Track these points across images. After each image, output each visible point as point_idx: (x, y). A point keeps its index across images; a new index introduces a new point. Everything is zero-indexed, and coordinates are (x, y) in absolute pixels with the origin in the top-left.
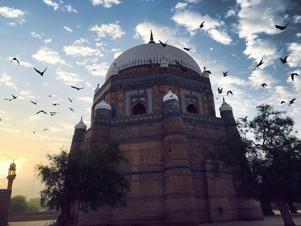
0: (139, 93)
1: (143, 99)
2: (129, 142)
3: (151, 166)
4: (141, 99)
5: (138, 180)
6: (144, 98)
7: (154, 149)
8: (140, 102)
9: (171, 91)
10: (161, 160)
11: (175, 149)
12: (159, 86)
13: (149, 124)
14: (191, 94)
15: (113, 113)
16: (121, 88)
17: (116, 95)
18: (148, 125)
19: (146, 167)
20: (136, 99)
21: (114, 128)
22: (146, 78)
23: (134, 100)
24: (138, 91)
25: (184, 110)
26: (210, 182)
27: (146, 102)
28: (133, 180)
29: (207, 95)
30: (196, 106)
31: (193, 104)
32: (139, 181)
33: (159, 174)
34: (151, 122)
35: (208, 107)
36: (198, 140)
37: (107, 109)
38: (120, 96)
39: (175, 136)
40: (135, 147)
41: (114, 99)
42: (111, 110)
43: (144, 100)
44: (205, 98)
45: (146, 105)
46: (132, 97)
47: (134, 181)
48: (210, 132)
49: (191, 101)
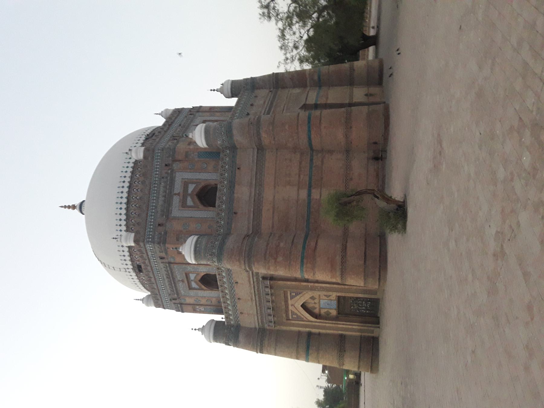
0: (179, 193)
6: (190, 185)
7: (276, 163)
8: (195, 193)
12: (175, 161)
18: (237, 171)
19: (302, 176)
20: (189, 199)
21: (233, 227)
23: (189, 202)
24: (175, 194)
27: (196, 182)
28: (318, 197)
32: (321, 189)
34: (235, 168)
37: (198, 238)
38: (176, 226)
40: (268, 194)
43: (194, 185)
44: (204, 114)
45: (203, 184)
46: (184, 205)
48: (262, 102)
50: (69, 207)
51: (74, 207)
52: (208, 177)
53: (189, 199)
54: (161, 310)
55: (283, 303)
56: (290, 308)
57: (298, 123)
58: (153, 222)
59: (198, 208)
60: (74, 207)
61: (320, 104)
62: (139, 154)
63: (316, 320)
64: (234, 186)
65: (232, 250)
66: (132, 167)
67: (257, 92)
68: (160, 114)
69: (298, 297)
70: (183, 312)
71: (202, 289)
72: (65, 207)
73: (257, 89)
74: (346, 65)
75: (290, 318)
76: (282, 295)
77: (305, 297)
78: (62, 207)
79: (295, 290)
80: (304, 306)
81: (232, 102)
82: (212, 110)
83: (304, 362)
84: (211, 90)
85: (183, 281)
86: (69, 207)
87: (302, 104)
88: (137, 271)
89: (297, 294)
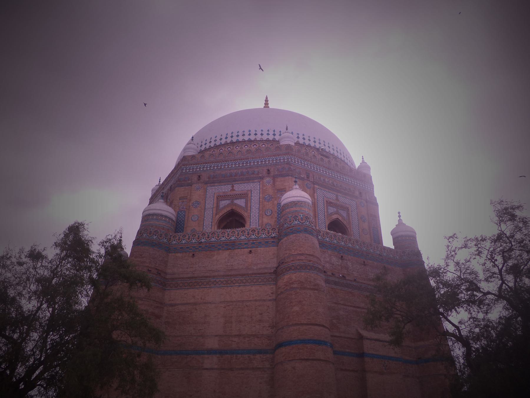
0: (235, 190)
1: (241, 202)
2: (205, 283)
3: (247, 339)
5: (216, 367)
7: (256, 300)
8: (234, 207)
9: (297, 186)
10: (269, 327)
11: (300, 301)
12: (274, 178)
13: (250, 249)
14: (337, 199)
15: (179, 225)
16: (199, 180)
18: (247, 250)
19: (236, 339)
20: (227, 202)
22: (250, 163)
23: (224, 203)
25: (324, 228)
30: (345, 223)
31: (340, 218)
33: (264, 357)
39: (303, 274)
41: (185, 200)
42: (174, 219)
43: (243, 205)
45: (245, 214)
46: (220, 198)
47: (207, 369)
49: (337, 213)
52: (253, 221)
53: (227, 202)
57: (302, 324)
58: (207, 170)
59: (216, 214)
62: (288, 140)
65: (141, 255)
68: (363, 162)
78: (267, 98)
81: (388, 242)
84: (399, 213)
87: (365, 333)
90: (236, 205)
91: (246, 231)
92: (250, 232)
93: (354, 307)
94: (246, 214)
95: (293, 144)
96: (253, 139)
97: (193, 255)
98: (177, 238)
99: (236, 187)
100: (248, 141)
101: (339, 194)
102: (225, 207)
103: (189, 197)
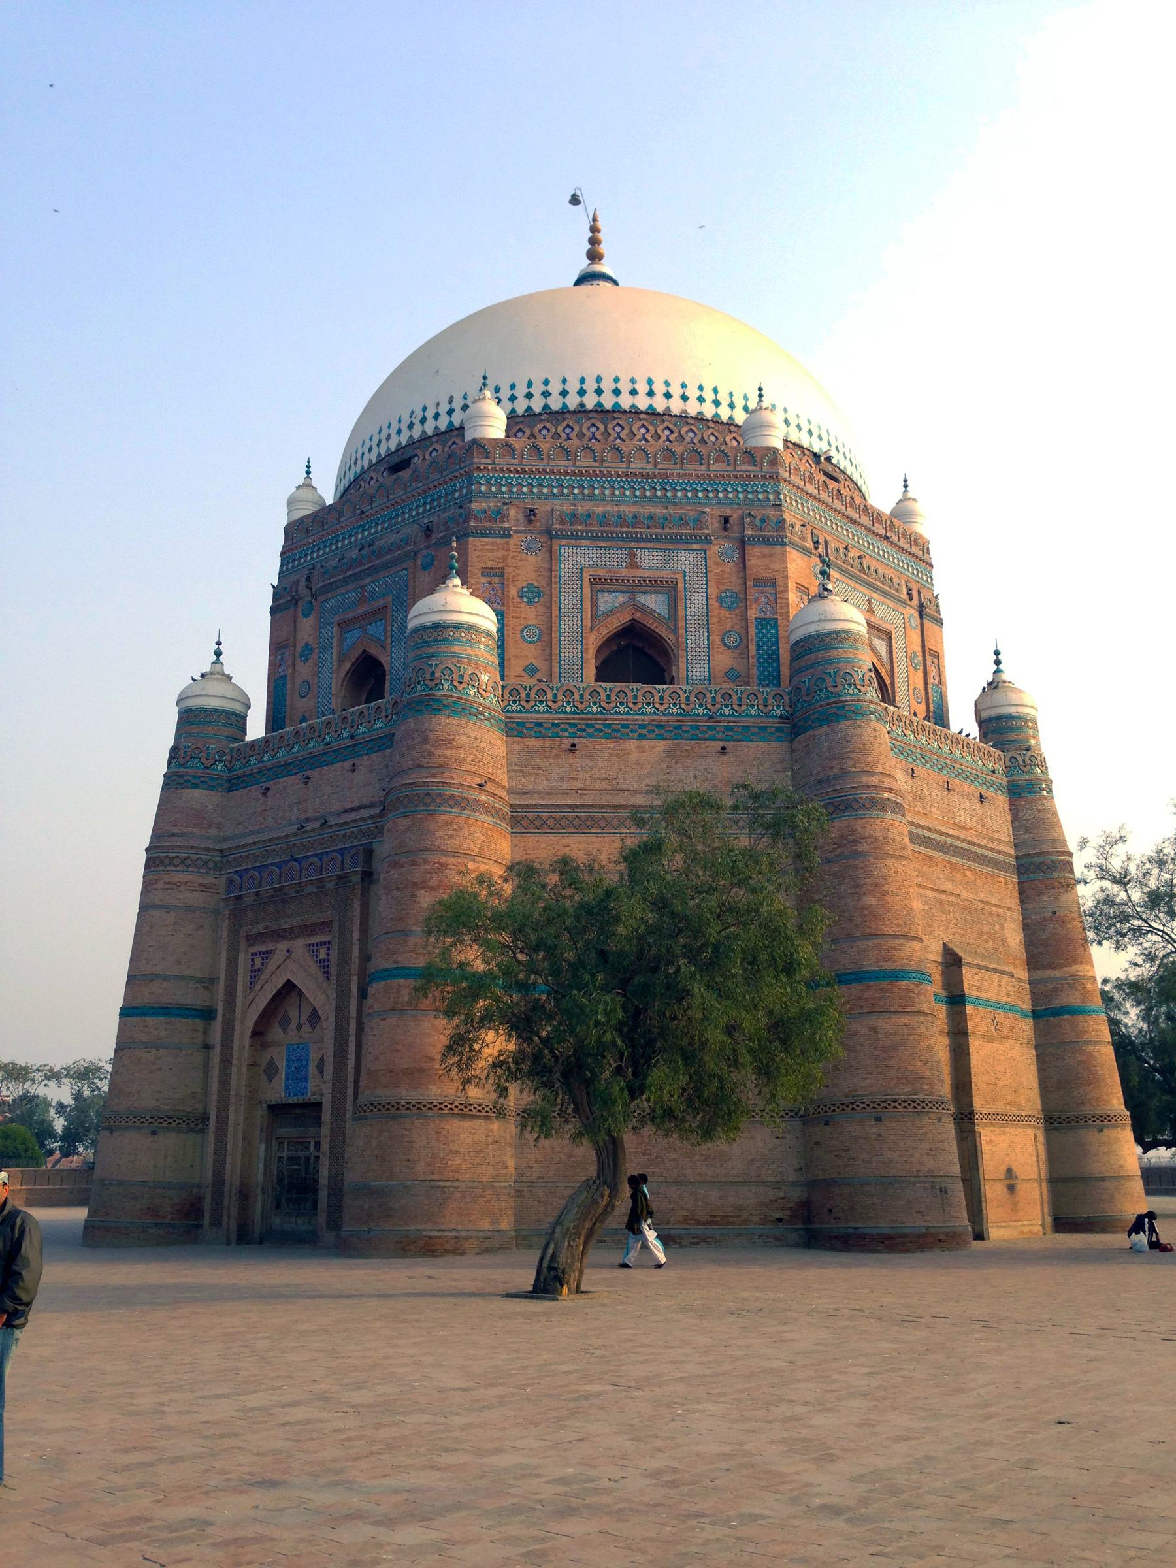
0: (637, 567)
4: (642, 599)
6: (662, 598)
8: (638, 616)
12: (742, 544)
13: (721, 744)
17: (504, 558)
20: (622, 598)
24: (632, 555)
26: (978, 1050)
29: (922, 625)
35: (926, 684)
36: (930, 852)
41: (496, 579)
44: (915, 637)
45: (669, 638)
46: (601, 584)
48: (962, 817)
50: (594, 241)
51: (594, 256)
54: (278, 541)
55: (296, 921)
56: (282, 946)
60: (594, 256)
61: (963, 1013)
63: (249, 1034)
64: (661, 737)
66: (717, 415)
67: (1001, 800)
69: (314, 969)
70: (273, 611)
71: (341, 662)
72: (594, 229)
73: (1012, 803)
74: (1116, 1102)
75: (254, 949)
76: (318, 917)
77: (318, 994)
79: (334, 958)
80: (289, 987)
82: (930, 658)
83: (120, 1002)
84: (997, 653)
85: (362, 600)
86: (594, 241)
88: (395, 459)
89: (324, 965)
90: (643, 609)
91: (709, 696)
92: (719, 699)
93: (936, 890)
94: (672, 637)
95: (780, 445)
96: (660, 409)
97: (573, 746)
98: (523, 695)
99: (642, 557)
100: (647, 413)
101: (875, 596)
102: (613, 611)
103: (508, 570)
